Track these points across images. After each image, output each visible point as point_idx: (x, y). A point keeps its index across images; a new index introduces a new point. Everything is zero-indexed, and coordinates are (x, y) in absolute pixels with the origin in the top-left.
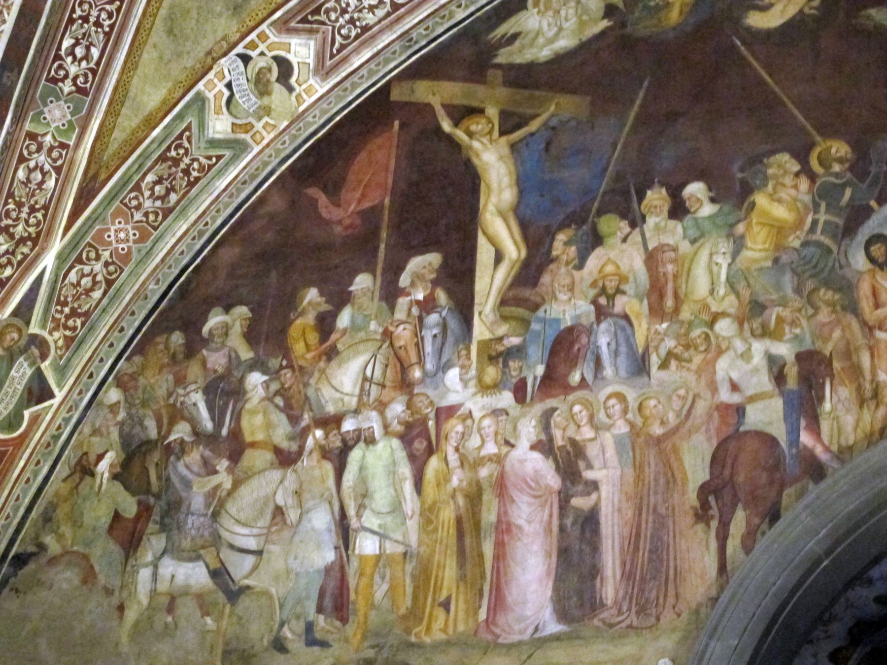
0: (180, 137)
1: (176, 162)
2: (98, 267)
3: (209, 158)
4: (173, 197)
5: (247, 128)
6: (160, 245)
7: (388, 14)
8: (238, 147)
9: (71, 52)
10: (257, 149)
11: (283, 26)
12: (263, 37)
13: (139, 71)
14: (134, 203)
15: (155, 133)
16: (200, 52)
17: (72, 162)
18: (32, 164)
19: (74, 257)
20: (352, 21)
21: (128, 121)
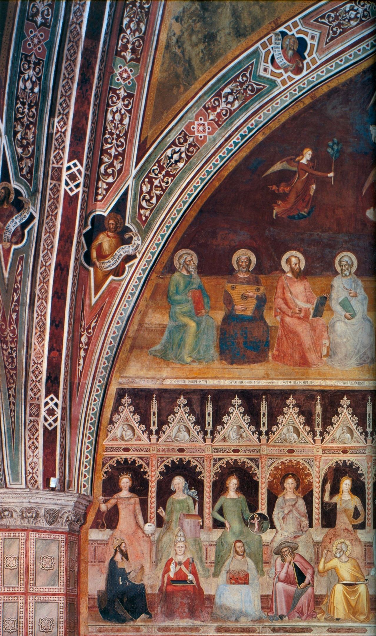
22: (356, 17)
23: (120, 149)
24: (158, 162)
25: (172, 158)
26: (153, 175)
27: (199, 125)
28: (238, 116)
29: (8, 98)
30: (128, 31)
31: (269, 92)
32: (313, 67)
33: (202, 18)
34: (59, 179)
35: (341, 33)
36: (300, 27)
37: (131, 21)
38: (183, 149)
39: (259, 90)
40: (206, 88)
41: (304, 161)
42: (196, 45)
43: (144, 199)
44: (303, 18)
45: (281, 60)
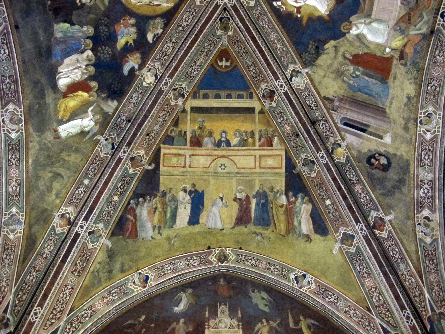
0: (424, 249)
1: (428, 254)
2: (436, 288)
3: (433, 248)
4: (435, 261)
5: (433, 235)
6: (442, 272)
7: (432, 190)
8: (436, 240)
9: (394, 254)
10: (439, 237)
11: (419, 212)
12: (418, 218)
13: (406, 245)
14: (430, 269)
15: (420, 253)
16: (411, 232)
17: (413, 272)
18: (407, 280)
19: (430, 290)
20: (428, 198)
21: (414, 255)
22: (170, 269)
23: (62, 309)
24: (77, 316)
25: (83, 315)
26: (73, 322)
27: (99, 303)
28: (116, 302)
29: (21, 281)
30: (79, 265)
31: (131, 294)
32: (151, 286)
33: (109, 264)
34: (29, 314)
35: (163, 275)
36: (147, 271)
37: (81, 261)
38: (89, 312)
39: (127, 293)
40: (105, 290)
41: (141, 320)
42: (104, 273)
43: (66, 331)
44: (149, 268)
45: (138, 282)
